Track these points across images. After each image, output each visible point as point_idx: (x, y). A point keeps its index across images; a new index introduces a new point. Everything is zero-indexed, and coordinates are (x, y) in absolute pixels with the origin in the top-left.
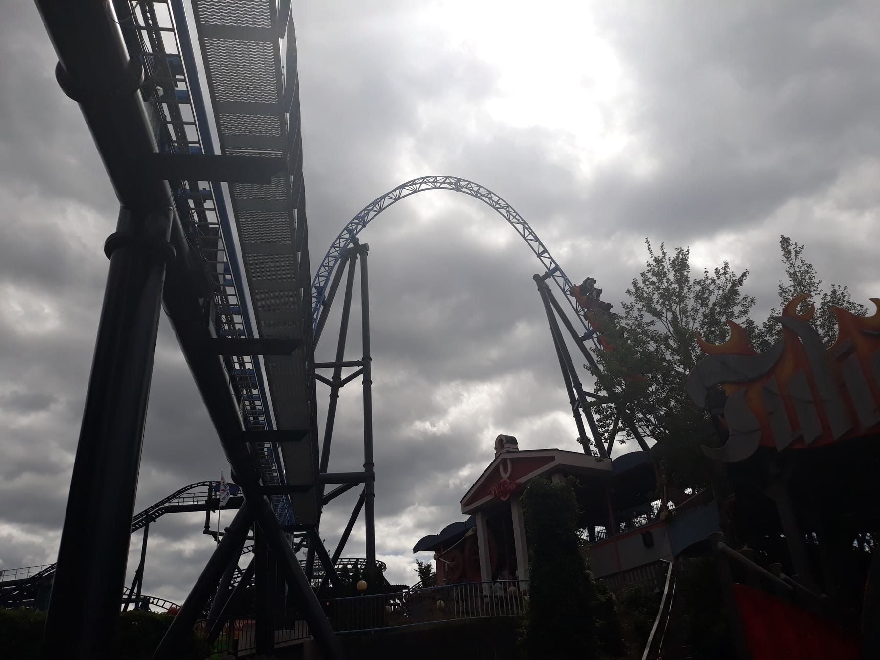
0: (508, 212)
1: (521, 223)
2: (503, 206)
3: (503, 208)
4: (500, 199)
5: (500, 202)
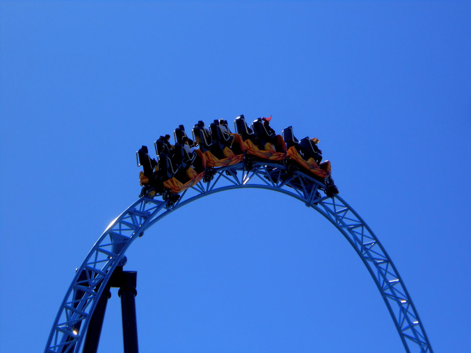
0: (402, 309)
1: (419, 342)
2: (374, 255)
3: (397, 299)
4: (377, 242)
5: (398, 287)
